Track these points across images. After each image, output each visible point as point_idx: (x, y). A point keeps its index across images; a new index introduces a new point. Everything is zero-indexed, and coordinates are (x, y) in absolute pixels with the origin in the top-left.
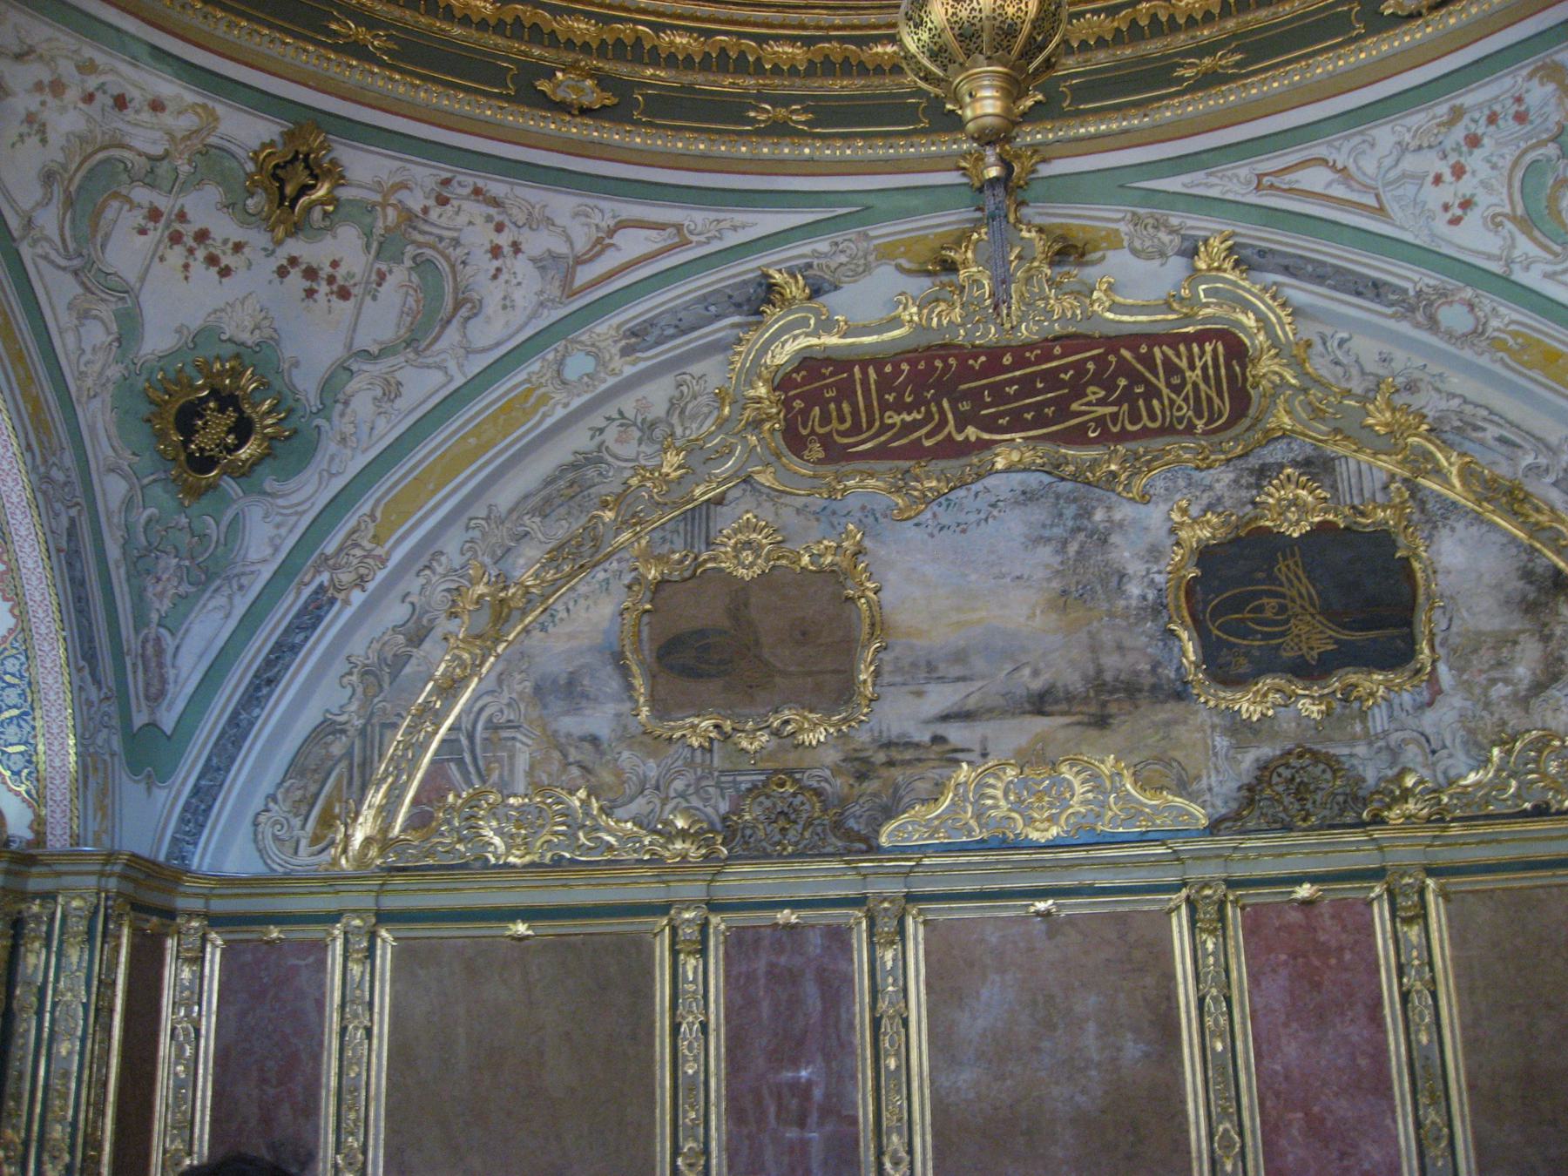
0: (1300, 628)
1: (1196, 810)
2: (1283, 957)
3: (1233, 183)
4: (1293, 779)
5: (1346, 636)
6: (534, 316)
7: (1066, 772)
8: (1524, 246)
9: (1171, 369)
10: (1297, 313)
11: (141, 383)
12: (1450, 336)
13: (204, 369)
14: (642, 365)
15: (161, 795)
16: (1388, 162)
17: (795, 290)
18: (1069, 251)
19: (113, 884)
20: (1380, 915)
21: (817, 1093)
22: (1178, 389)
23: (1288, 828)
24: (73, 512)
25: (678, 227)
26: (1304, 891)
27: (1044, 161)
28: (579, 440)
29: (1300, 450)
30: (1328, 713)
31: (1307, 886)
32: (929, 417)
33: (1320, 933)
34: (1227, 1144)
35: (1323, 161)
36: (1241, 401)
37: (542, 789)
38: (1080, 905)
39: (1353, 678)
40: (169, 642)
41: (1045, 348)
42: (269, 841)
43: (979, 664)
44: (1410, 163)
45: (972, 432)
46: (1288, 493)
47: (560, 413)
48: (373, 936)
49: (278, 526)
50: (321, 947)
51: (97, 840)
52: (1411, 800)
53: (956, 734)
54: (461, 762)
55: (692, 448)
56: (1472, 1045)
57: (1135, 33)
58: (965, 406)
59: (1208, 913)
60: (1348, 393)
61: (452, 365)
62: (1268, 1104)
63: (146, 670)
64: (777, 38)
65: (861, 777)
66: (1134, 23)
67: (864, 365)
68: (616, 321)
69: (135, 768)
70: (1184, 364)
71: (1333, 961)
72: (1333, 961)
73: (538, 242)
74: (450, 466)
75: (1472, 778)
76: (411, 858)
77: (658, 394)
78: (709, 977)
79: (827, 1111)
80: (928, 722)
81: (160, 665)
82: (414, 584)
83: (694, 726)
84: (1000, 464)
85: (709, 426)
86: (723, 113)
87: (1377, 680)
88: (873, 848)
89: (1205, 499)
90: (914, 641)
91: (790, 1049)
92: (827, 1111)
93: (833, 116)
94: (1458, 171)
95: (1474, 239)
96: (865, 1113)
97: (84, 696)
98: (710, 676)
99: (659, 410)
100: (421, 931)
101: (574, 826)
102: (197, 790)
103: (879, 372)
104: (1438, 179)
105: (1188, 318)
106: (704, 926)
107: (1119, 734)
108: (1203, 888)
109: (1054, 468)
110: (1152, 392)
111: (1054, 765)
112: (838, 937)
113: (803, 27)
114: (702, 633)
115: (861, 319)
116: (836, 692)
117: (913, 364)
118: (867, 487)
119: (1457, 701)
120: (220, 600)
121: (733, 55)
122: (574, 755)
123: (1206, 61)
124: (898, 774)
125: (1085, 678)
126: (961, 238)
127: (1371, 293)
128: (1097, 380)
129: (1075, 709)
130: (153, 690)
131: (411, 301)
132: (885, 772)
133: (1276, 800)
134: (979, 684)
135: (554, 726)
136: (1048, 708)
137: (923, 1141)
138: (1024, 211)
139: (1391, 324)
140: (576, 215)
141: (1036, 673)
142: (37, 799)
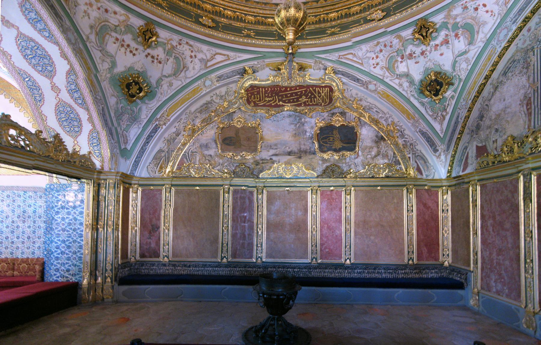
0: (336, 143)
1: (315, 173)
3: (334, 56)
5: (344, 145)
6: (199, 71)
7: (293, 166)
8: (387, 74)
9: (319, 93)
10: (343, 83)
11: (117, 77)
12: (370, 91)
13: (131, 76)
14: (220, 84)
15: (128, 162)
16: (364, 54)
17: (250, 71)
18: (302, 68)
20: (343, 193)
21: (247, 218)
22: (320, 97)
23: (330, 178)
25: (228, 56)
26: (332, 188)
27: (299, 48)
28: (208, 98)
29: (340, 110)
30: (339, 158)
32: (273, 99)
34: (314, 229)
35: (352, 54)
36: (331, 100)
37: (201, 164)
39: (344, 153)
41: (296, 87)
42: (150, 171)
43: (279, 146)
44: (368, 55)
45: (281, 103)
46: (337, 118)
47: (204, 92)
48: (171, 189)
50: (161, 191)
51: (115, 169)
53: (274, 158)
54: (186, 158)
55: (230, 102)
56: (356, 216)
57: (319, 22)
58: (280, 98)
59: (314, 191)
60: (350, 100)
61: (183, 80)
64: (249, 15)
66: (320, 19)
67: (262, 88)
68: (215, 74)
70: (321, 92)
73: (200, 56)
74: (183, 101)
75: (362, 171)
76: (177, 175)
77: (223, 90)
78: (229, 197)
79: (249, 221)
84: (286, 109)
85: (233, 97)
86: (238, 31)
87: (348, 153)
88: (258, 178)
89: (322, 118)
91: (243, 210)
92: (249, 221)
93: (259, 34)
94: (377, 57)
95: (377, 72)
96: (255, 221)
99: (223, 93)
100: (180, 188)
101: (207, 171)
102: (135, 161)
103: (265, 89)
104: (373, 58)
105: (323, 83)
106: (229, 189)
107: (303, 160)
109: (295, 111)
110: (315, 97)
111: (291, 165)
113: (254, 13)
114: (230, 138)
115: (262, 78)
116: (254, 150)
117: (271, 88)
118: (261, 112)
119: (361, 158)
121: (240, 18)
122: (207, 158)
123: (333, 30)
124: (264, 165)
126: (282, 64)
127: (357, 81)
128: (304, 95)
131: (174, 66)
133: (329, 173)
137: (265, 226)
138: (294, 59)
139: (360, 87)
140: (207, 51)
142: (102, 161)
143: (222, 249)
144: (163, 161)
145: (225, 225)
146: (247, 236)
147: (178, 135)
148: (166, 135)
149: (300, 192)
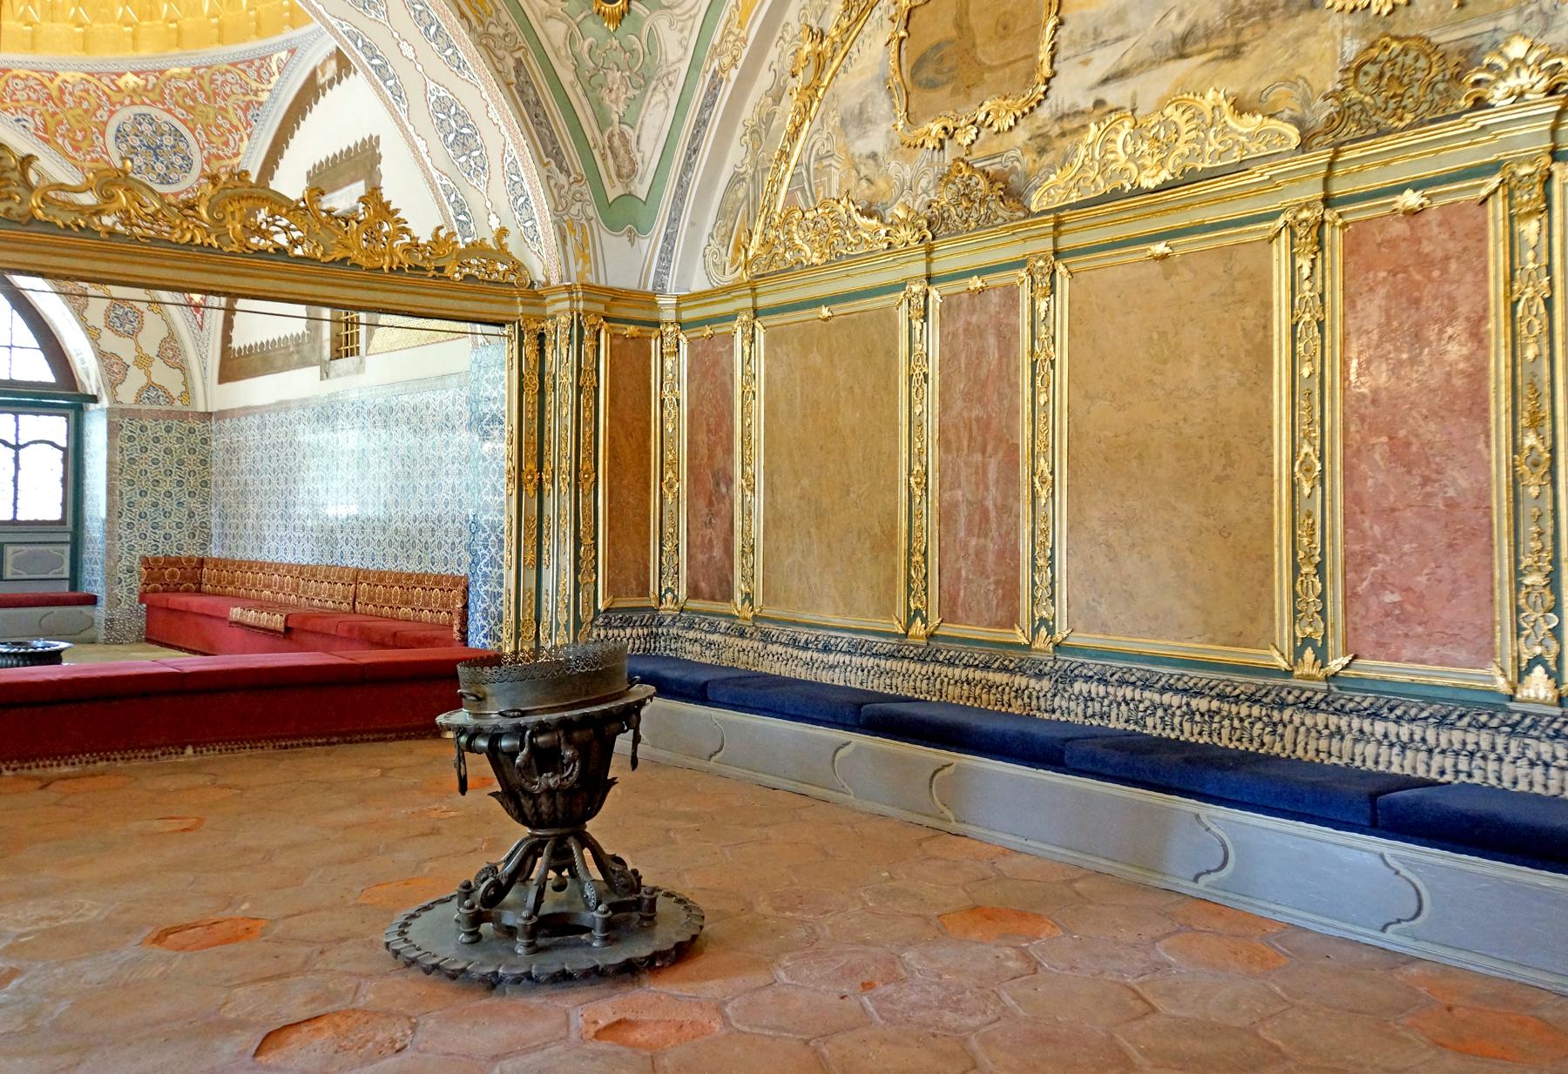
2: (1383, 274)
4: (1381, 76)
15: (644, 243)
19: (581, 305)
24: (518, 54)
26: (1411, 199)
31: (1409, 192)
33: (1425, 243)
38: (1190, 243)
40: (631, 134)
49: (681, 31)
50: (730, 337)
52: (1524, 73)
53: (1114, 95)
54: (803, 190)
62: (1353, 428)
63: (615, 156)
65: (1041, 151)
69: (613, 227)
71: (1436, 274)
72: (1436, 274)
80: (1092, 88)
81: (628, 152)
82: (772, 54)
83: (929, 133)
90: (1085, 10)
97: (552, 183)
98: (944, 84)
102: (666, 239)
108: (1301, 210)
112: (1011, 293)
114: (938, 47)
120: (659, 96)
122: (864, 171)
124: (1066, 143)
125: (1224, 9)
129: (1214, 43)
130: (625, 171)
132: (1058, 144)
134: (1132, 40)
135: (852, 150)
136: (1188, 50)
141: (1181, 15)
143: (909, 579)
144: (742, 222)
145: (917, 467)
146: (993, 515)
147: (777, 100)
148: (748, 113)
149: (1227, 253)
